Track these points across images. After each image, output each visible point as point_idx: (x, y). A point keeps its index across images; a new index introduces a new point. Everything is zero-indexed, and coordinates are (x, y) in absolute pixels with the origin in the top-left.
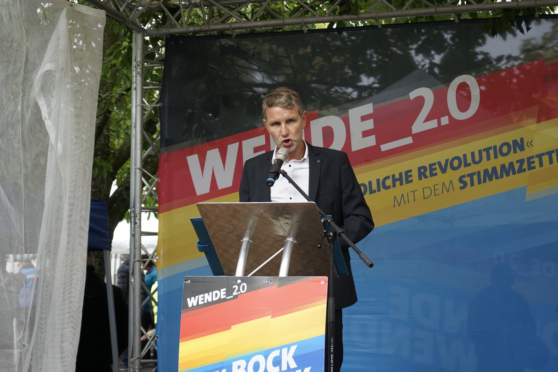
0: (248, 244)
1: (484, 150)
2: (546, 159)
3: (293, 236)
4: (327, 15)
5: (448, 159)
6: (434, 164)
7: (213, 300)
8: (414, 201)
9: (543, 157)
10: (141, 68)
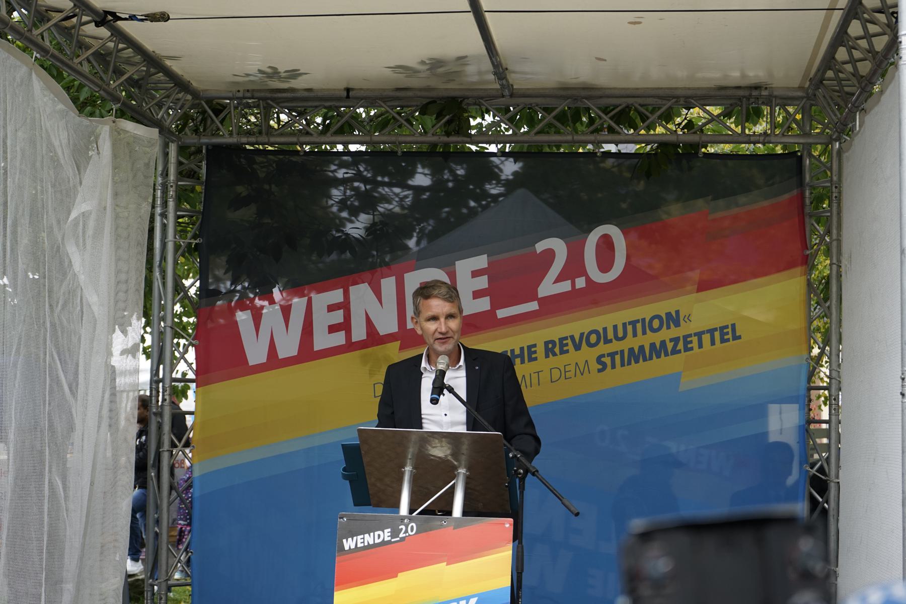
0: (411, 475)
1: (630, 323)
2: (706, 338)
3: (465, 467)
4: (430, 135)
5: (584, 333)
6: (566, 338)
7: (376, 542)
8: (539, 385)
9: (703, 336)
10: (174, 190)
